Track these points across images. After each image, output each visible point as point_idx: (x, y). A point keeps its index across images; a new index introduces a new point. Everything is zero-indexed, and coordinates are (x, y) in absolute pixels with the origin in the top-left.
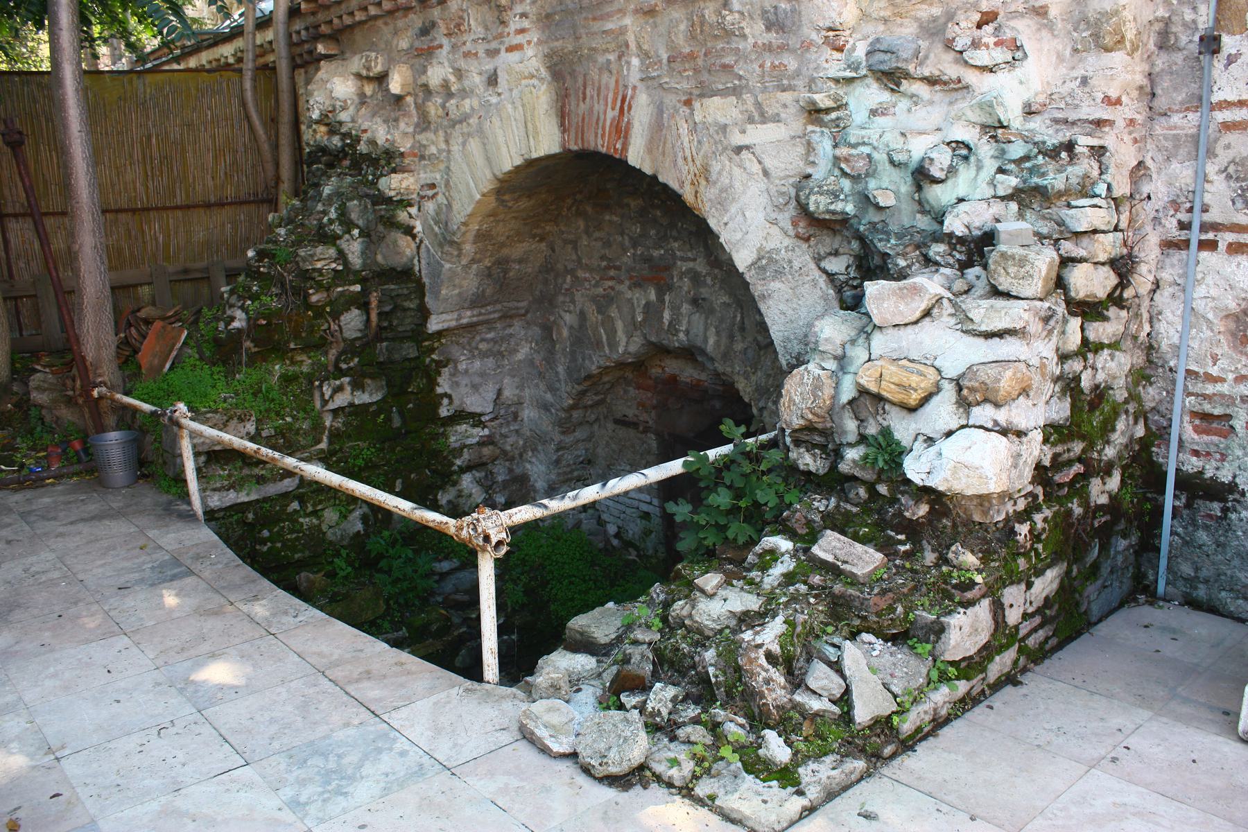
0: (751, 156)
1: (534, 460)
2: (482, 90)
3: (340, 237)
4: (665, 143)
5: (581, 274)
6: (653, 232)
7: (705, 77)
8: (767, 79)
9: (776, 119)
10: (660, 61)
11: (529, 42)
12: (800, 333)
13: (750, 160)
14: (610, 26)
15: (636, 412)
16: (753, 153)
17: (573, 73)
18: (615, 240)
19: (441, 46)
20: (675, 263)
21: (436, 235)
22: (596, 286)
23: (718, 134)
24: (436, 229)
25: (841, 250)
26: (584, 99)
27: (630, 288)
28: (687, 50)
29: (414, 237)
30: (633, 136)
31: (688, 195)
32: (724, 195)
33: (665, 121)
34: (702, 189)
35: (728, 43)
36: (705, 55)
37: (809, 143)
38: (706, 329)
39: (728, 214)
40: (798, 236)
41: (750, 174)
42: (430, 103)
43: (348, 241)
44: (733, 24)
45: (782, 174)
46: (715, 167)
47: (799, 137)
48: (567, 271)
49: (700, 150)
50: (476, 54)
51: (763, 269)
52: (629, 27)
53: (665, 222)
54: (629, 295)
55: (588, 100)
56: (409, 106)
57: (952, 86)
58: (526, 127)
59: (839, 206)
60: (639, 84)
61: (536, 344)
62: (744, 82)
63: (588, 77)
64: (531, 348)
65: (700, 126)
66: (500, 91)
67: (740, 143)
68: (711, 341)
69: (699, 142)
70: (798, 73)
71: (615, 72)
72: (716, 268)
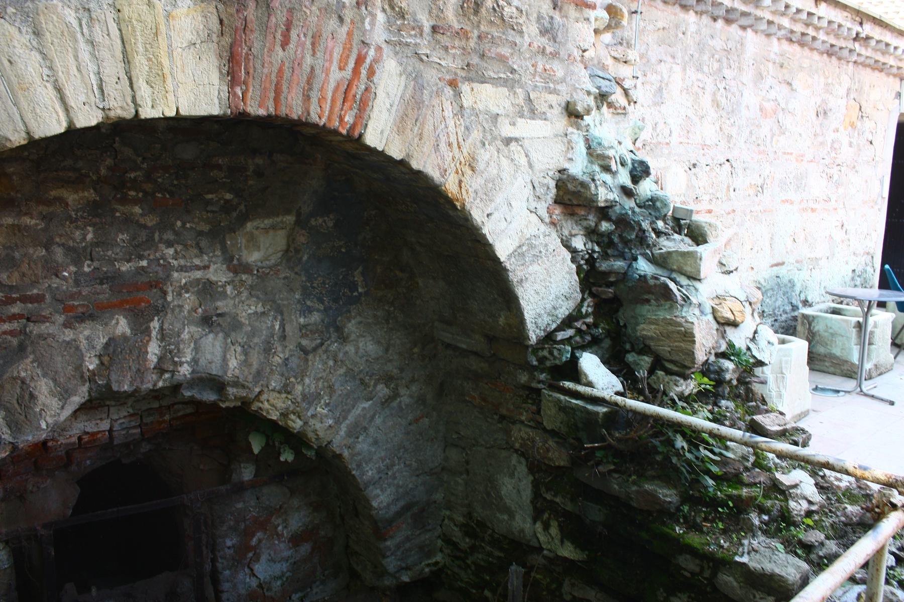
0: (519, 148)
4: (423, 124)
6: (122, 237)
7: (475, 60)
8: (537, 78)
9: (544, 117)
10: (421, 28)
12: (549, 306)
13: (519, 152)
16: (521, 146)
20: (169, 276)
23: (488, 122)
25: (573, 232)
26: (285, 44)
27: (67, 325)
28: (457, 26)
30: (376, 109)
31: (451, 186)
32: (490, 185)
33: (426, 97)
34: (466, 179)
35: (504, 33)
36: (479, 37)
37: (570, 142)
39: (493, 205)
40: (553, 224)
41: (517, 167)
44: (511, 18)
45: (543, 167)
46: (484, 156)
47: (561, 136)
49: (468, 137)
51: (523, 255)
53: (151, 221)
54: (69, 335)
57: (620, 111)
58: (127, 60)
59: (611, 196)
60: (384, 46)
62: (517, 77)
63: (297, 15)
65: (468, 111)
67: (509, 136)
68: (233, 363)
69: (467, 128)
70: (563, 80)
71: (348, 20)
72: (244, 273)
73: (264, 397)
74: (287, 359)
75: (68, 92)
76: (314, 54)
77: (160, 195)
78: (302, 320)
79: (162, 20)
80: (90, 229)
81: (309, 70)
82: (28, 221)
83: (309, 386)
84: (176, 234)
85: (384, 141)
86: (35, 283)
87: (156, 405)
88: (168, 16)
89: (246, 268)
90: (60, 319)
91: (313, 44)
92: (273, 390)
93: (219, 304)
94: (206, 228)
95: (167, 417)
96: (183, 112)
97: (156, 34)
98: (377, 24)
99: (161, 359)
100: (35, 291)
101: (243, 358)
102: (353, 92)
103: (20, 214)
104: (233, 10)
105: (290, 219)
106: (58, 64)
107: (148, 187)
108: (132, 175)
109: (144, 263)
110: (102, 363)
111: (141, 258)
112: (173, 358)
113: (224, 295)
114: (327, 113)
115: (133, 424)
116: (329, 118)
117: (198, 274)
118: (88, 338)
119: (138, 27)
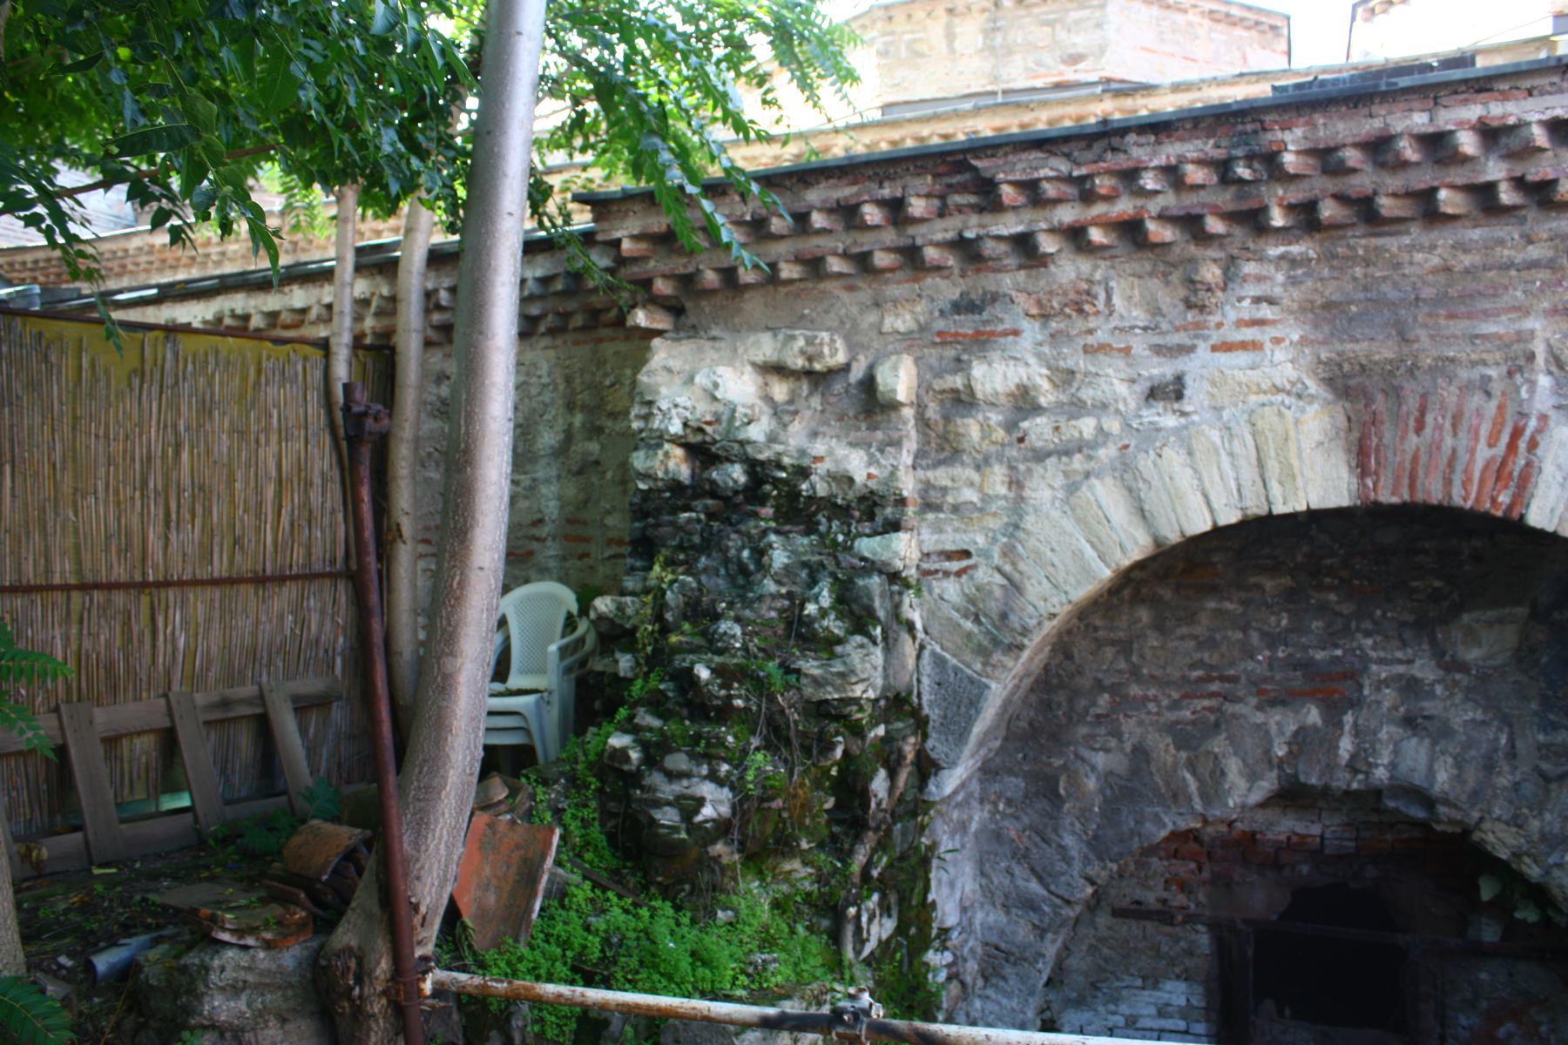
1: (990, 992)
2: (1132, 405)
3: (840, 641)
5: (1135, 690)
6: (1317, 624)
11: (1277, 341)
14: (1490, 328)
15: (1165, 895)
17: (1395, 393)
18: (1225, 637)
19: (1016, 333)
20: (1366, 669)
21: (969, 635)
22: (1175, 705)
24: (968, 625)
26: (1420, 427)
27: (1259, 708)
29: (914, 638)
30: (1541, 485)
38: (1432, 760)
42: (970, 421)
43: (862, 646)
48: (1099, 686)
50: (1127, 351)
52: (1539, 333)
53: (1347, 609)
54: (1259, 718)
55: (1428, 431)
56: (905, 423)
58: (1261, 464)
60: (1552, 413)
61: (1009, 802)
64: (995, 811)
66: (1188, 408)
73: (1487, 825)
74: (1517, 784)
75: (1212, 498)
76: (1455, 434)
77: (1356, 582)
78: (1541, 737)
79: (1291, 427)
80: (1285, 615)
81: (1449, 452)
82: (1229, 606)
83: (1550, 823)
84: (1376, 623)
85: (1556, 521)
86: (1232, 664)
87: (1375, 818)
88: (1297, 422)
89: (1463, 667)
90: (1253, 701)
91: (1454, 426)
92: (1499, 819)
93: (1426, 704)
94: (1410, 618)
95: (1389, 837)
96: (1314, 506)
97: (1286, 440)
98: (1539, 390)
99: (1354, 757)
100: (1232, 672)
101: (1455, 772)
102: (1507, 470)
103: (1222, 599)
104: (1361, 406)
105: (1522, 611)
106: (1205, 474)
107: (1344, 574)
108: (1328, 562)
109: (1339, 652)
110: (1290, 752)
111: (1336, 646)
112: (1366, 759)
113: (1431, 695)
114: (1473, 495)
115: (1347, 835)
116: (1477, 500)
117: (1401, 669)
118: (1278, 723)
119: (1270, 435)
